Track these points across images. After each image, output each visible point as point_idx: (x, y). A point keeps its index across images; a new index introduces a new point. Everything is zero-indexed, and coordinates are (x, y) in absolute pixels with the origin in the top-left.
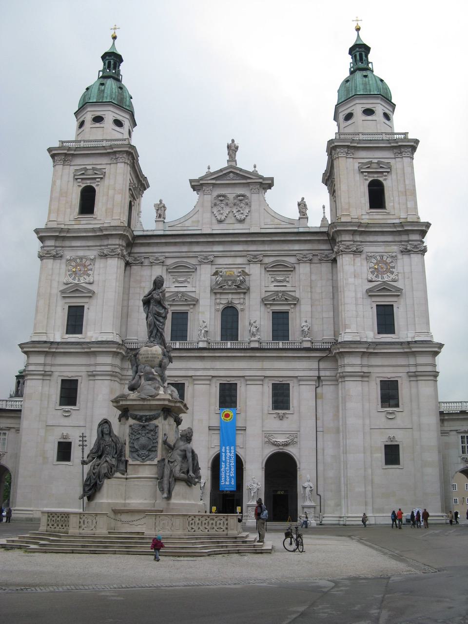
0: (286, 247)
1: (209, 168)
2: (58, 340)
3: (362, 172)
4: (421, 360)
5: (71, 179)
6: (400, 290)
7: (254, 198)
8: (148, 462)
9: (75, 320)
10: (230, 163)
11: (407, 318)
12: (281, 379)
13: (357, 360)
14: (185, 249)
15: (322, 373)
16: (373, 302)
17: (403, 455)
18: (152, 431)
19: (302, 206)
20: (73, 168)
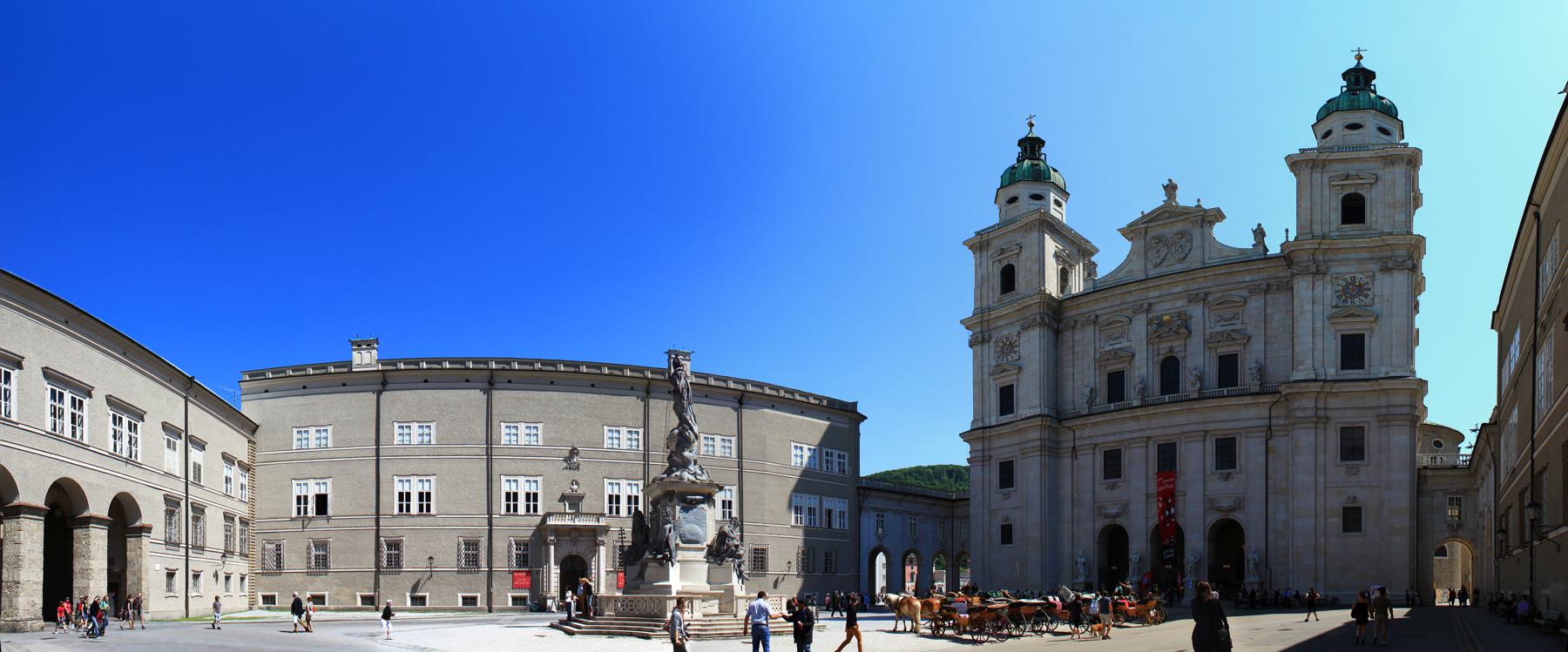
7: (1197, 232)
19: (1259, 233)
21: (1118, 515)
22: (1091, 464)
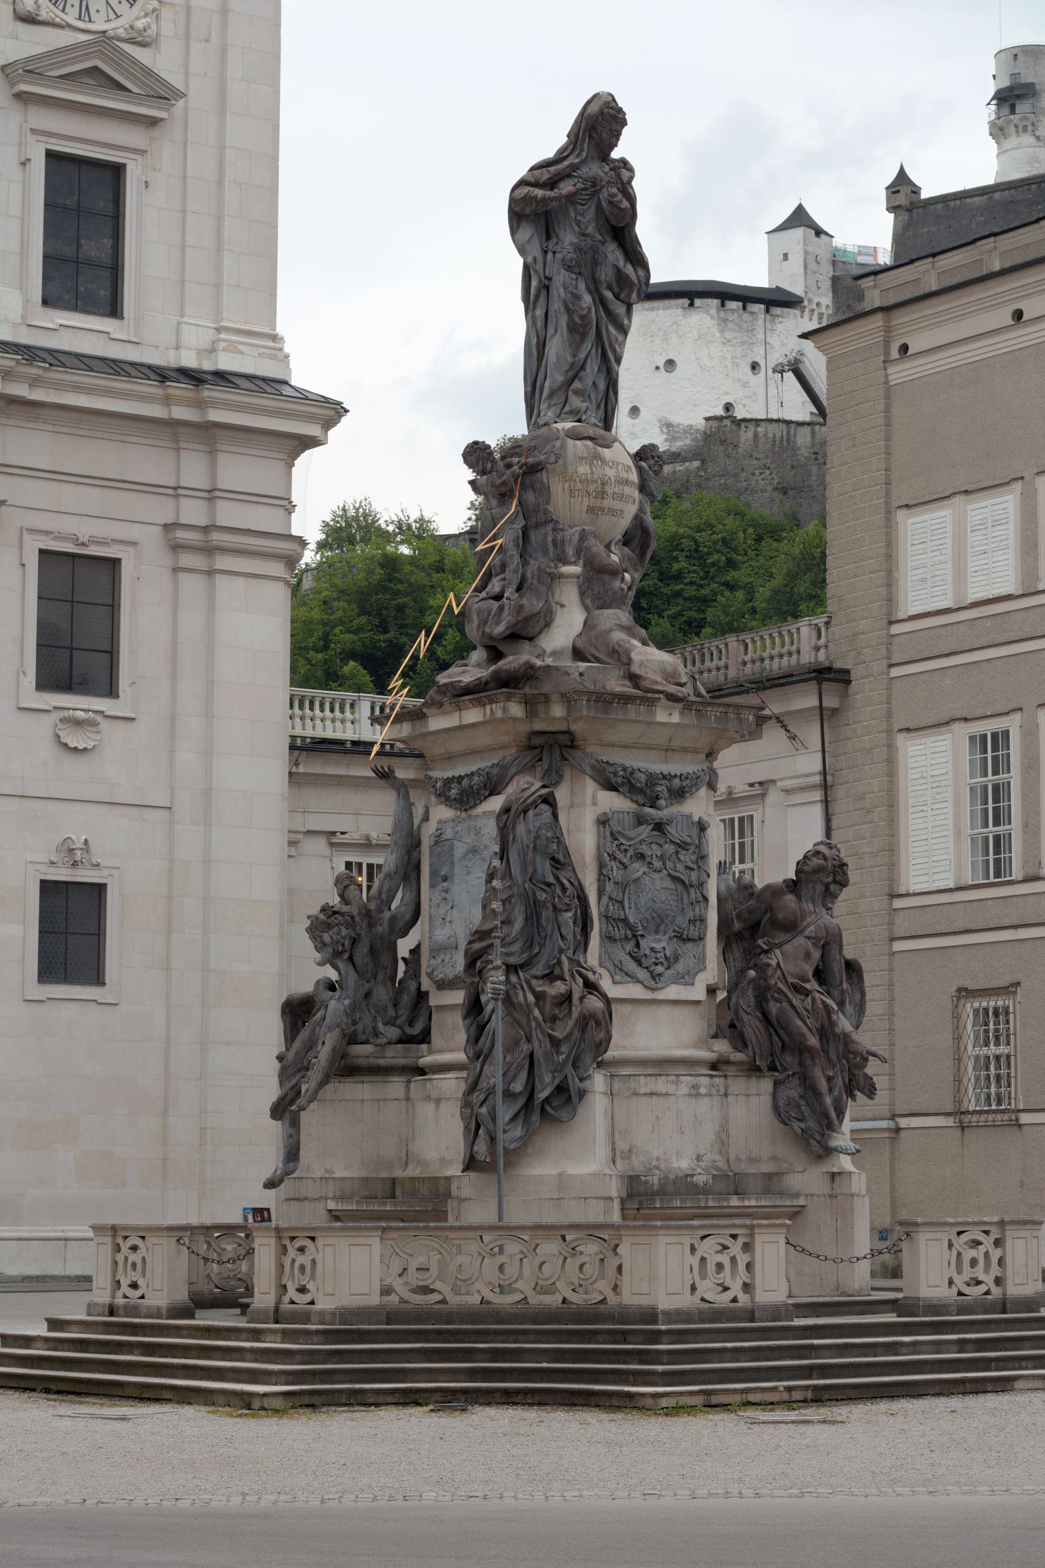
4: (239, 470)
6: (165, 94)
8: (673, 992)
11: (184, 247)
16: (34, 131)
18: (682, 846)
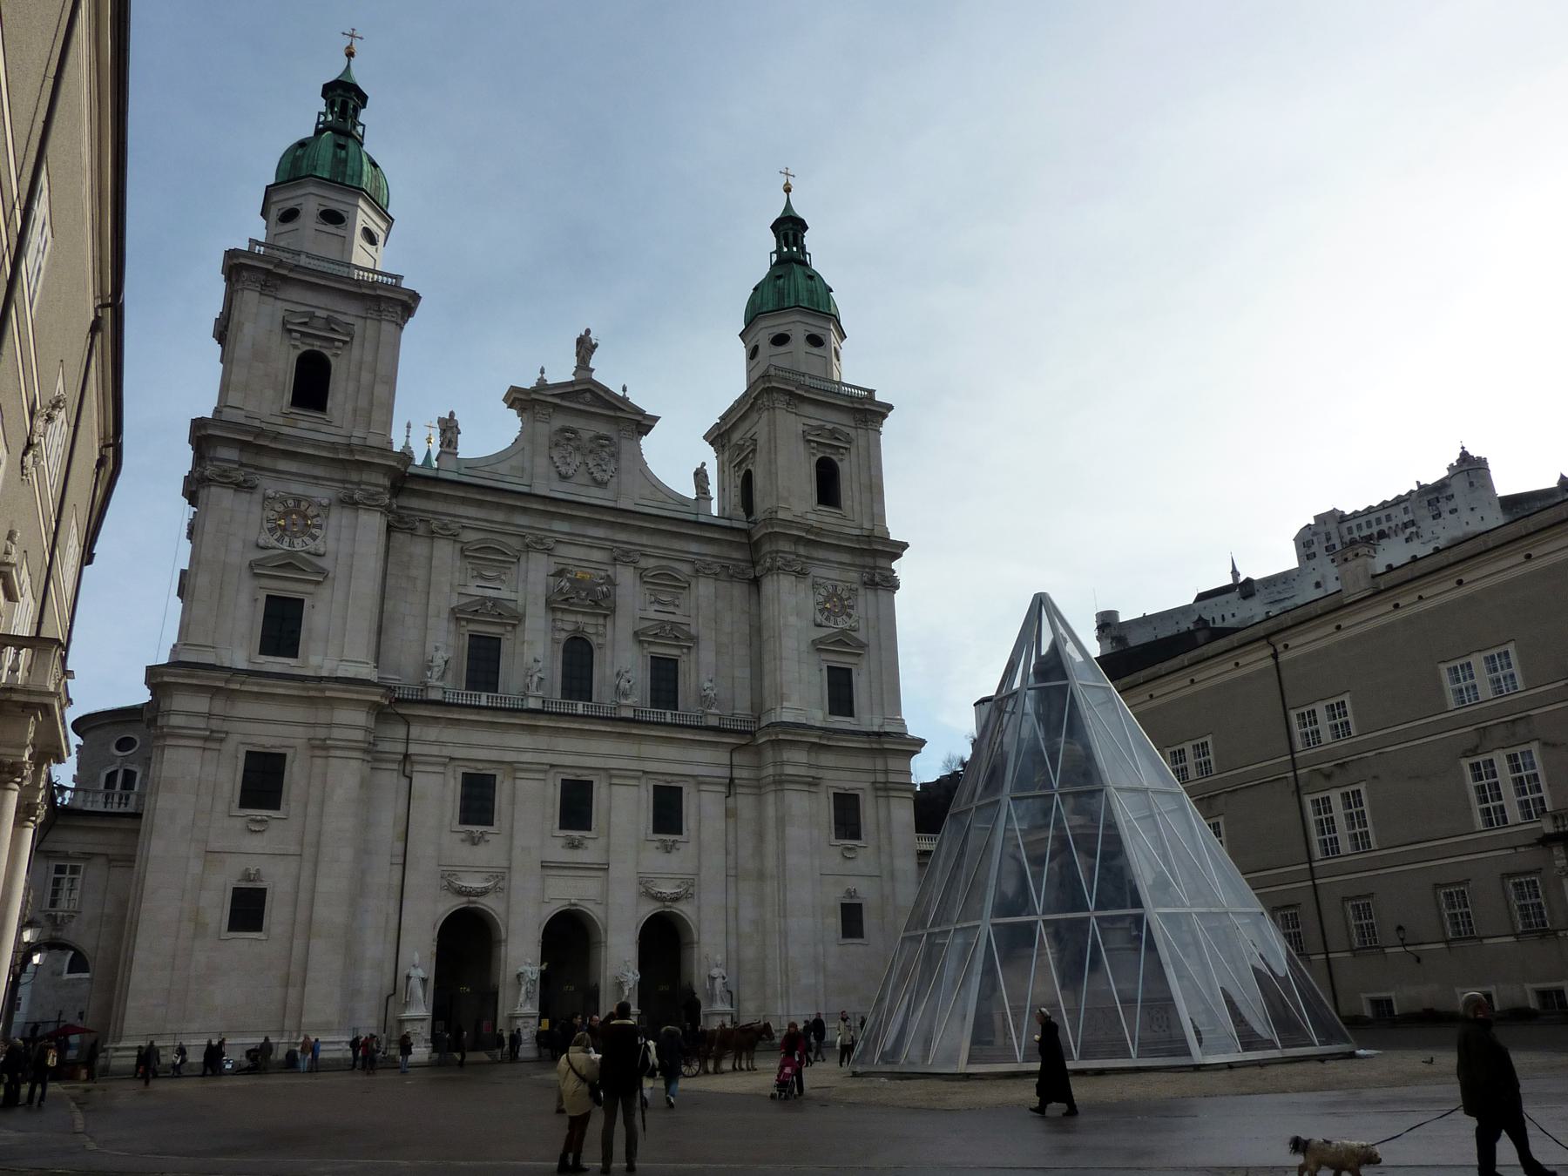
0: (678, 544)
1: (542, 371)
2: (241, 664)
3: (809, 441)
4: (894, 763)
5: (278, 328)
6: (862, 646)
7: (625, 445)
9: (282, 626)
10: (584, 374)
12: (669, 778)
13: (800, 756)
14: (499, 516)
15: (737, 773)
17: (869, 921)
20: (279, 304)
21: (484, 892)
22: (439, 794)
